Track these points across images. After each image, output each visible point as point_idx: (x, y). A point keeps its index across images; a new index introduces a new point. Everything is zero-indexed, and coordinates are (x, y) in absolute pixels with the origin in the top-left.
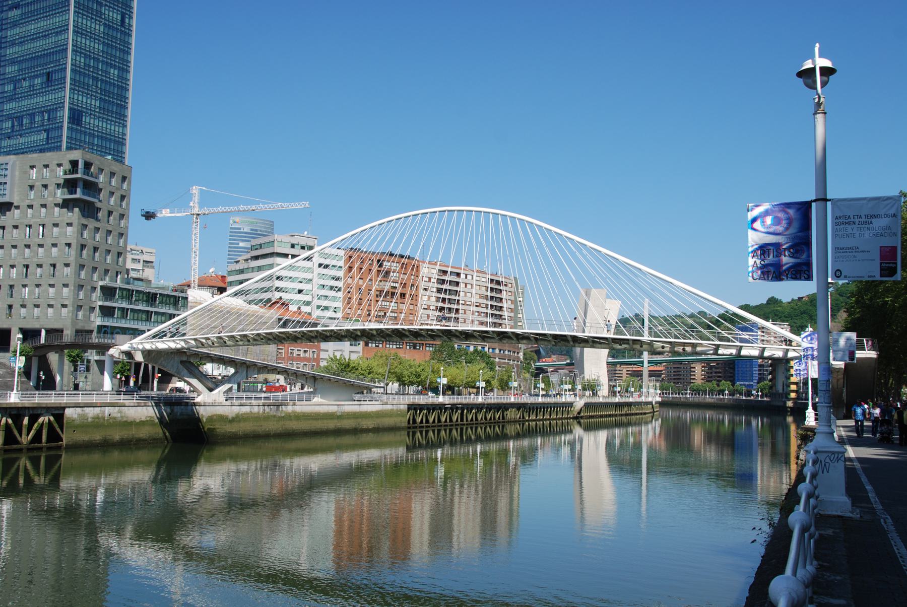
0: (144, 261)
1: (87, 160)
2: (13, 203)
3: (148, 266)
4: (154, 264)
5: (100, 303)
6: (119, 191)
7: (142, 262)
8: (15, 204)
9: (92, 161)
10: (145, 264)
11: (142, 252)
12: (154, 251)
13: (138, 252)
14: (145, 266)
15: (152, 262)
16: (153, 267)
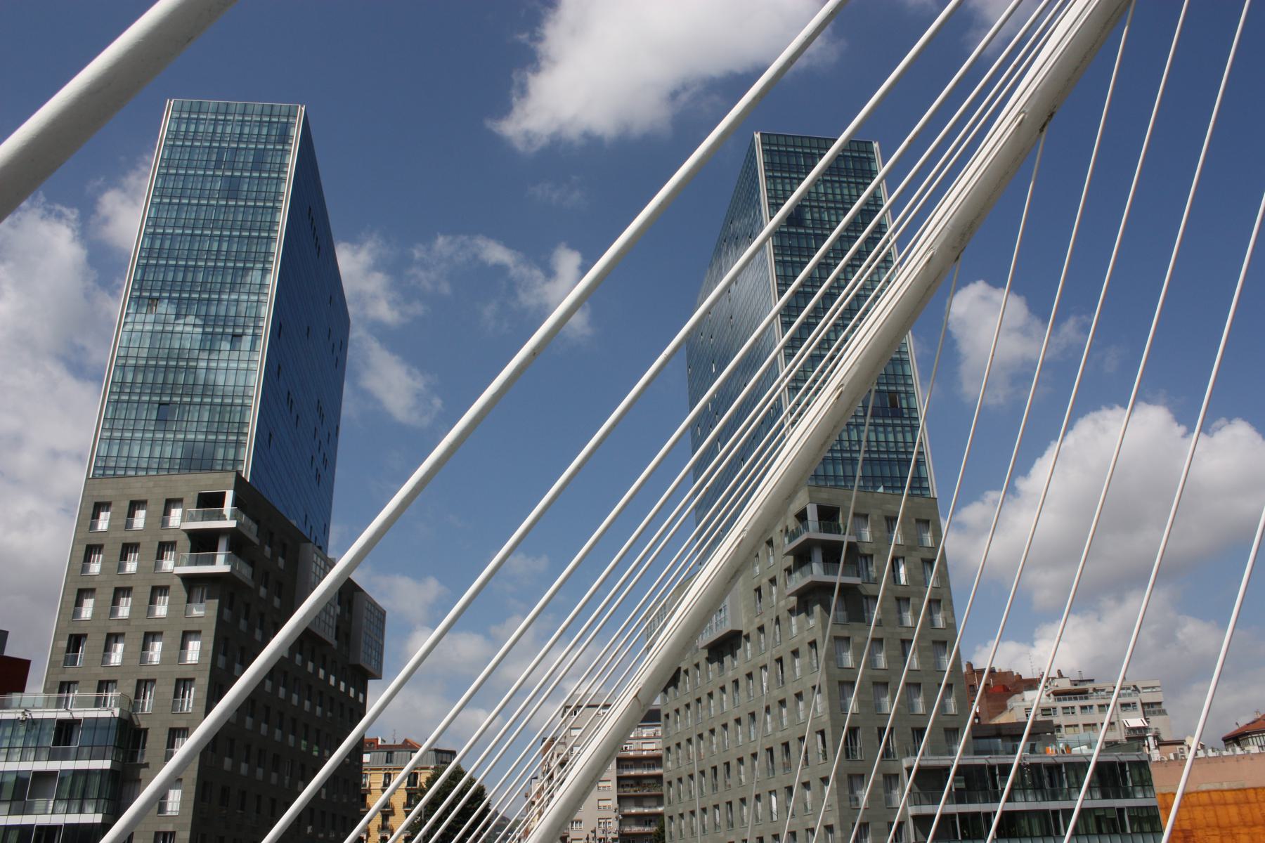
0: (1143, 704)
1: (824, 503)
2: (741, 632)
3: (1154, 713)
4: (1163, 706)
5: (912, 811)
6: (914, 553)
7: (1139, 706)
8: (745, 633)
9: (835, 504)
10: (1146, 709)
11: (1136, 689)
12: (1156, 683)
13: (1129, 691)
14: (1149, 713)
15: (1159, 703)
16: (1163, 712)
